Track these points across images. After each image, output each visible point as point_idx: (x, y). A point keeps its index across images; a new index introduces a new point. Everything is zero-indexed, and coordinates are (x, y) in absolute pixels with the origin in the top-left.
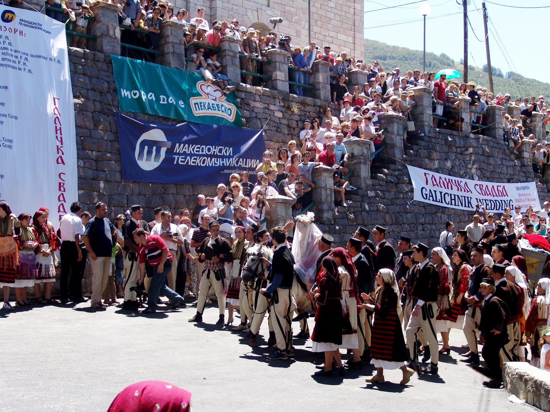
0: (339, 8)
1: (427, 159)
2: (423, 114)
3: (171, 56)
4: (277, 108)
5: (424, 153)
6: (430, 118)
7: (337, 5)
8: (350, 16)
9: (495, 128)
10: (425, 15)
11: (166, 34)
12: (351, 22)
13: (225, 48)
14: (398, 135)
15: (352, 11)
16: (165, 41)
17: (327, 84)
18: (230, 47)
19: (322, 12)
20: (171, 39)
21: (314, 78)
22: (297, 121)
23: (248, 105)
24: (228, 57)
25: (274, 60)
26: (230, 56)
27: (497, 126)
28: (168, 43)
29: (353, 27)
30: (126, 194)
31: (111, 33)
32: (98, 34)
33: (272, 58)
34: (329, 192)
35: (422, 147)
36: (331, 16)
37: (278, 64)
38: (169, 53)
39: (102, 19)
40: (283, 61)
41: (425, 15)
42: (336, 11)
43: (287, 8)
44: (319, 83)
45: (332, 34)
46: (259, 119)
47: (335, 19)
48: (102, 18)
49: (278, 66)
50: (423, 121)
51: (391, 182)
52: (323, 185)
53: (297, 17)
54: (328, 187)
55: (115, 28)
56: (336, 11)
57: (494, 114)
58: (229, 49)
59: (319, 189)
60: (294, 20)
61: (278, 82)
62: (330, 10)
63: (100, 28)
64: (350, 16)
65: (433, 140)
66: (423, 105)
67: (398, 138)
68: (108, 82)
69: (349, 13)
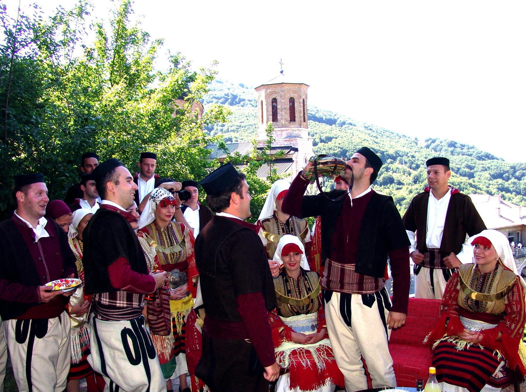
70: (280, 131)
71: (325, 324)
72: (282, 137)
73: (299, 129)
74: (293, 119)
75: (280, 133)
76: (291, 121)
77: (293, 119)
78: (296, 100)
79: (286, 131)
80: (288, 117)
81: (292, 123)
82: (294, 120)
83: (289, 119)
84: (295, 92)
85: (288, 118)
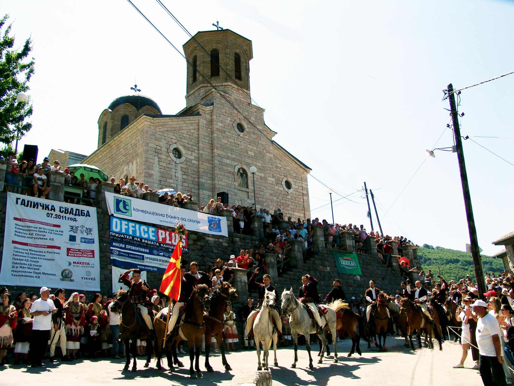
0: (294, 199)
1: (321, 266)
2: (317, 240)
4: (225, 241)
5: (318, 262)
6: (323, 243)
7: (293, 197)
8: (301, 203)
9: (371, 249)
10: (331, 194)
12: (302, 206)
14: (299, 251)
15: (302, 200)
17: (261, 228)
18: (192, 207)
19: (283, 201)
21: (253, 225)
22: (239, 248)
23: (204, 239)
27: (372, 248)
29: (303, 209)
34: (243, 284)
35: (317, 259)
36: (290, 203)
41: (331, 194)
42: (292, 201)
43: (260, 199)
44: (255, 227)
45: (290, 212)
46: (211, 247)
47: (292, 205)
50: (318, 244)
51: (294, 279)
52: (239, 279)
53: (266, 204)
54: (243, 281)
56: (292, 201)
57: (370, 241)
58: (191, 208)
59: (237, 282)
60: (264, 205)
62: (288, 200)
64: (301, 203)
65: (326, 255)
66: (317, 235)
67: (298, 253)
68: (103, 225)
69: (300, 201)
70: (198, 91)
71: (28, 195)
72: (199, 97)
73: (224, 84)
74: (215, 71)
75: (198, 93)
76: (212, 75)
77: (215, 71)
78: (220, 52)
79: (204, 88)
80: (208, 71)
81: (213, 78)
82: (218, 74)
83: (210, 74)
84: (218, 42)
85: (208, 73)
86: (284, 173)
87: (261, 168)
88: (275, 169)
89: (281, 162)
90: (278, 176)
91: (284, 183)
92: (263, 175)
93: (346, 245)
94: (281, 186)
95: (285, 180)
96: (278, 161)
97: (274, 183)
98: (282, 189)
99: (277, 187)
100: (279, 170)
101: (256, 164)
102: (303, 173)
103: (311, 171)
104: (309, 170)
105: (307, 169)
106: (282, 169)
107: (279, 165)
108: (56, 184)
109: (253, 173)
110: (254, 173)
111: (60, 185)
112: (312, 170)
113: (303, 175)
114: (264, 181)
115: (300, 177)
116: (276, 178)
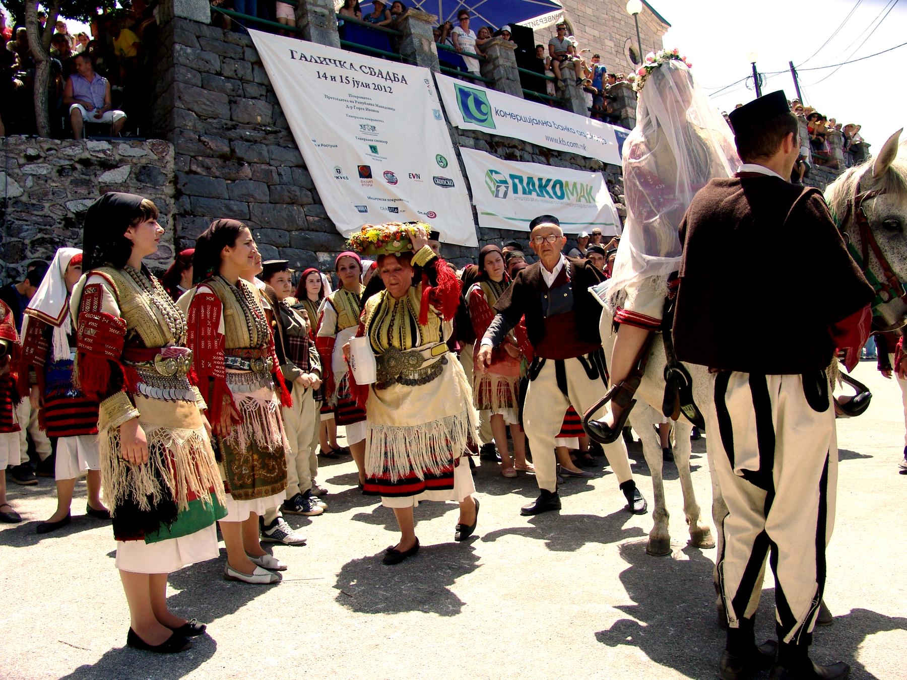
3: (503, 80)
11: (494, 57)
13: (565, 77)
16: (494, 65)
20: (501, 61)
24: (570, 87)
25: (620, 95)
26: (573, 86)
28: (498, 66)
30: (473, 257)
31: (426, 48)
32: (409, 51)
33: (618, 94)
37: (626, 98)
38: (501, 78)
39: (413, 31)
40: (631, 96)
48: (412, 30)
49: (626, 102)
55: (430, 44)
61: (630, 120)
63: (412, 42)
86: (626, 32)
87: (593, 18)
88: (611, 23)
89: (620, 9)
90: (618, 37)
91: (627, 53)
92: (596, 33)
93: (836, 159)
94: (624, 57)
95: (627, 46)
96: (614, 7)
97: (614, 52)
98: (625, 64)
99: (617, 60)
100: (617, 25)
101: (583, 10)
102: (655, 33)
103: (669, 29)
104: (666, 26)
105: (663, 24)
106: (623, 23)
107: (618, 16)
108: (318, 10)
109: (635, 14)
110: (637, 13)
111: (326, 12)
112: (670, 26)
113: (655, 36)
114: (598, 46)
115: (652, 40)
116: (614, 42)
